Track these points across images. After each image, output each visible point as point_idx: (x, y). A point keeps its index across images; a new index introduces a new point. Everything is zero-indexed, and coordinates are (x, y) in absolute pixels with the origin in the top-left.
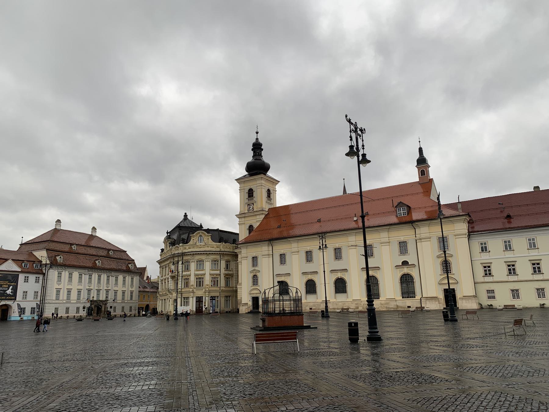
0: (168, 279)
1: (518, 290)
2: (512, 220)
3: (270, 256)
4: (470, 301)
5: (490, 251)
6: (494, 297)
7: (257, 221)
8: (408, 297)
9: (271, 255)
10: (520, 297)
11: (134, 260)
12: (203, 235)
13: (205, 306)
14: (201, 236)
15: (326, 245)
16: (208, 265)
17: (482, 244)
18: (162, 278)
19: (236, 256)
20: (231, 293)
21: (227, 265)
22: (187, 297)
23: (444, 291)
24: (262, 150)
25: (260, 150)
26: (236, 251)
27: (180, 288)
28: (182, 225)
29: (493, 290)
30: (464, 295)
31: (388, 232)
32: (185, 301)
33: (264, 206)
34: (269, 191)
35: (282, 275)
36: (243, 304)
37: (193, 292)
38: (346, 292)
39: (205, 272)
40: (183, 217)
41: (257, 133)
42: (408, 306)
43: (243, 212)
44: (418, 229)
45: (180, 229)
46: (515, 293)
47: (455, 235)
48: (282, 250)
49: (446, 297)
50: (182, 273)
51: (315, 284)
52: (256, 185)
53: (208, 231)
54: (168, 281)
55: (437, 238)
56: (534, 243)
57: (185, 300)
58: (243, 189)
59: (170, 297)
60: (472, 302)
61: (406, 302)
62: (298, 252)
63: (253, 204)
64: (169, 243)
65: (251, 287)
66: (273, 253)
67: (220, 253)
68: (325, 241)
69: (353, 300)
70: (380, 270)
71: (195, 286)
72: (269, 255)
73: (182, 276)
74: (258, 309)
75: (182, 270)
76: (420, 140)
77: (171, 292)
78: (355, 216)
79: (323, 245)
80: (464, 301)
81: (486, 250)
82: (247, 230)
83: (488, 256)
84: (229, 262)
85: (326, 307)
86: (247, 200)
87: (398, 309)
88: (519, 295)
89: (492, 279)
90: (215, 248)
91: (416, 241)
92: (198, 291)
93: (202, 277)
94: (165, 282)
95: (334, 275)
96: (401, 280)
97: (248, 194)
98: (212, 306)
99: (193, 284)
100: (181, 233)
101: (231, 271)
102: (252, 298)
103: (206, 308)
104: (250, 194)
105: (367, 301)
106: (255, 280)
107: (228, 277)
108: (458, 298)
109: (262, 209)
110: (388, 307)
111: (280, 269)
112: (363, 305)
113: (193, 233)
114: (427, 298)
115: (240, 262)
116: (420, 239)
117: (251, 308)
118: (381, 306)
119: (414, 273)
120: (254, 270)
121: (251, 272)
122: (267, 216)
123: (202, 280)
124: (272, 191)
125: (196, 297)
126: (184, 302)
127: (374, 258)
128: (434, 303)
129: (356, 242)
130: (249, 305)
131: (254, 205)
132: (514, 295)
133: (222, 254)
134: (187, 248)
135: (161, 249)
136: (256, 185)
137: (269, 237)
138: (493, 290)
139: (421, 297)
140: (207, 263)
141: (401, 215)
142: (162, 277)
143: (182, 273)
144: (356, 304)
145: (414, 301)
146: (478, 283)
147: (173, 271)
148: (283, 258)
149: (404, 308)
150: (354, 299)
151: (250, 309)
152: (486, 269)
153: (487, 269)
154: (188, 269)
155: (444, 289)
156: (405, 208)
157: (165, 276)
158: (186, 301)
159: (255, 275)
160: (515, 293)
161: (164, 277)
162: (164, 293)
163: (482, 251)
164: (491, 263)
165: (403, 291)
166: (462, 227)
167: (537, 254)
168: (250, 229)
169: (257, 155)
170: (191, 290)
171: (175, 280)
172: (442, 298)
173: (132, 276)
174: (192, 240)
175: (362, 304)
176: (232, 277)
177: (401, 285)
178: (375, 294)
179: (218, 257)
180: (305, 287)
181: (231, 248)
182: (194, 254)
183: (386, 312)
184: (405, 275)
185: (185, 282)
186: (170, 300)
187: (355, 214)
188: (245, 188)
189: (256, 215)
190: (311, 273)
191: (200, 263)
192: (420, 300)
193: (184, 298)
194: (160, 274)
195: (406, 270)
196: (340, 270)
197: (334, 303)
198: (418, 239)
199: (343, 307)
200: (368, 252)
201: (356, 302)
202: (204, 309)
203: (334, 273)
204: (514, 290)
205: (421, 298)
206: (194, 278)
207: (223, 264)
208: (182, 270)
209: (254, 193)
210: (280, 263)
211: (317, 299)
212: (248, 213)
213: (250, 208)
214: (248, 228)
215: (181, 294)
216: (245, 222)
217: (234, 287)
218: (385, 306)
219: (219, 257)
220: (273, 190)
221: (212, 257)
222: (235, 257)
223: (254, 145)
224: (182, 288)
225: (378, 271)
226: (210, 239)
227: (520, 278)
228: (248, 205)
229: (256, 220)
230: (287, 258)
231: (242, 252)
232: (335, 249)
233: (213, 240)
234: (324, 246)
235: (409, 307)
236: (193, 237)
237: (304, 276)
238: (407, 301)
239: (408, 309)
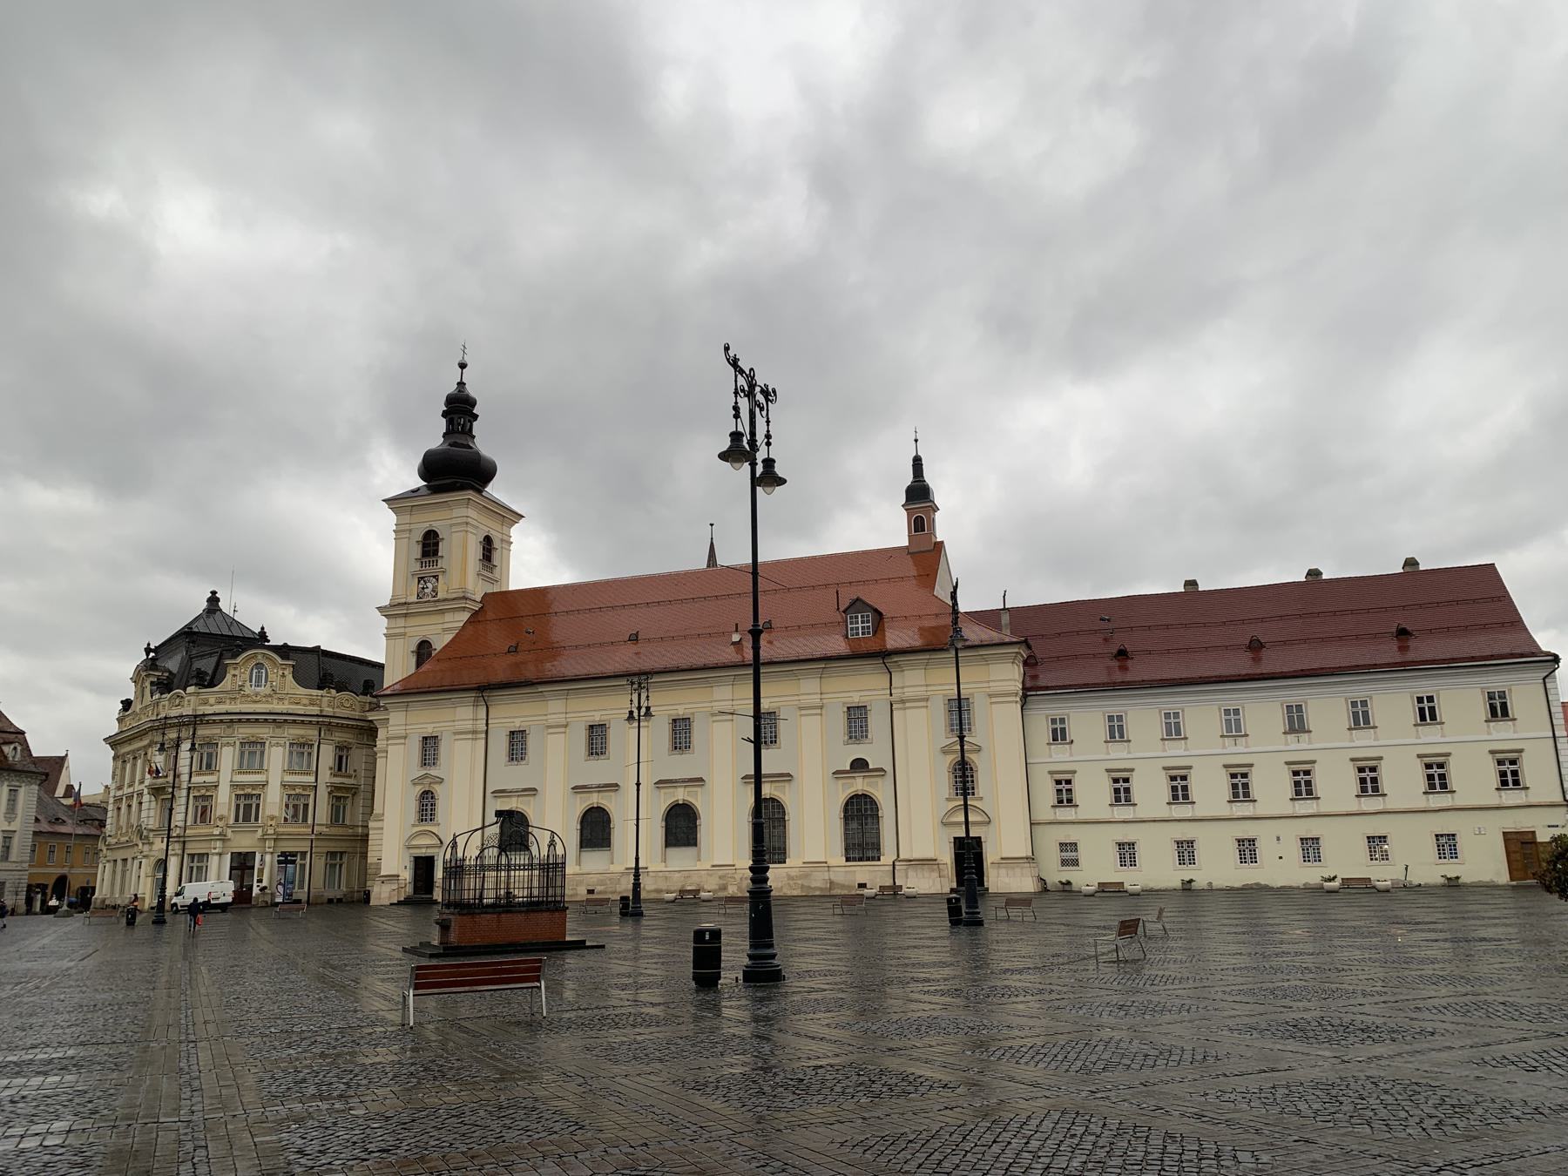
0: (140, 794)
1: (1253, 841)
2: (1129, 663)
3: (479, 736)
4: (1018, 870)
5: (1072, 741)
6: (1075, 862)
7: (444, 630)
8: (861, 859)
9: (481, 732)
10: (1137, 863)
11: (23, 733)
12: (267, 664)
13: (260, 881)
14: (259, 666)
15: (648, 708)
16: (276, 758)
17: (1054, 721)
18: (120, 793)
19: (369, 732)
20: (344, 844)
21: (341, 758)
22: (203, 854)
23: (955, 843)
24: (475, 417)
25: (468, 418)
26: (371, 716)
27: (181, 824)
28: (200, 628)
29: (1076, 844)
30: (1004, 856)
31: (820, 678)
32: (195, 864)
33: (470, 587)
34: (488, 540)
35: (511, 792)
36: (383, 876)
37: (223, 838)
38: (695, 845)
39: (267, 777)
40: (204, 605)
41: (463, 366)
42: (859, 884)
43: (403, 601)
44: (897, 673)
45: (193, 642)
46: (1127, 853)
47: (990, 696)
48: (515, 720)
49: (959, 859)
50: (191, 777)
51: (609, 821)
52: (450, 522)
53: (285, 651)
54: (141, 803)
55: (944, 700)
56: (1177, 724)
57: (193, 862)
58: (407, 530)
59: (145, 854)
60: (1022, 874)
61: (855, 871)
62: (566, 726)
63: (434, 577)
64: (152, 683)
65: (413, 825)
66: (490, 726)
67: (318, 722)
68: (648, 697)
69: (713, 866)
70: (793, 783)
71: (232, 821)
72: (474, 732)
73: (189, 788)
74: (431, 893)
76: (918, 438)
77: (147, 837)
78: (737, 631)
79: (639, 708)
80: (1003, 871)
81: (1064, 738)
83: (1068, 754)
84: (348, 749)
85: (637, 885)
86: (419, 564)
87: (834, 892)
88: (1257, 852)
89: (1073, 813)
90: (305, 705)
91: (892, 705)
92: (238, 836)
93: (254, 792)
94: (129, 806)
95: (665, 793)
96: (846, 810)
97: (420, 546)
98: (282, 881)
99: (225, 813)
100: (194, 652)
101: (350, 777)
102: (412, 859)
103: (263, 889)
104: (429, 545)
105: (751, 869)
106: (427, 805)
107: (341, 796)
108: (989, 862)
109: (462, 595)
110: (806, 884)
111: (507, 776)
112: (741, 879)
113: (235, 656)
114: (910, 861)
115: (382, 752)
116: (903, 702)
117: (409, 890)
118: (789, 884)
119: (881, 792)
120: (426, 776)
121: (415, 783)
122: (476, 617)
123: (254, 802)
124: (496, 544)
125: (232, 853)
126: (192, 868)
127: (872, 743)
128: (926, 874)
129: (734, 703)
130: (400, 881)
131: (437, 580)
132: (1183, 856)
133: (325, 724)
134: (212, 701)
135: (122, 702)
136: (450, 522)
137: (481, 678)
138: (1076, 844)
139: (896, 858)
141: (857, 634)
142: (120, 788)
143: (191, 777)
144: (720, 878)
145: (876, 868)
146: (1039, 824)
147: (158, 771)
148: (517, 743)
149: (849, 887)
150: (715, 863)
151: (405, 891)
152: (1060, 787)
153: (1064, 786)
154: (210, 766)
155: (955, 838)
156: (868, 616)
157: (130, 786)
158: (197, 867)
159: (426, 792)
160: (1127, 853)
161: (127, 790)
162: (124, 839)
163: (1055, 739)
164: (1075, 772)
165: (850, 841)
166: (1008, 674)
167: (1182, 752)
168: (422, 651)
169: (458, 432)
170: (217, 831)
171: (163, 799)
172: (949, 862)
173: (13, 783)
174: (229, 677)
175: (738, 877)
176: (353, 795)
177: (846, 824)
178: (774, 849)
179: (312, 733)
180: (579, 827)
181: (358, 707)
182: (234, 720)
183: (802, 899)
184: (856, 796)
185: (197, 807)
186: (143, 861)
187: (737, 625)
188: (412, 526)
189: (442, 612)
190: (599, 787)
191: (252, 751)
192: (891, 868)
193: (192, 856)
194: (113, 778)
195: (859, 784)
196: (684, 781)
197: (661, 874)
198: (897, 702)
199: (683, 886)
200: (763, 732)
201: (720, 873)
202: (256, 891)
203: (666, 790)
204: (1243, 841)
205: (894, 862)
206: (230, 797)
207: (327, 755)
208: (191, 768)
209: (440, 544)
210: (507, 758)
211: (612, 863)
212: (417, 603)
213: (426, 590)
215: (182, 845)
216: (407, 630)
217: (358, 826)
218: (799, 882)
219: (316, 733)
220: (502, 540)
221: (291, 731)
222: (368, 736)
223: (450, 400)
224: (188, 824)
225: (787, 784)
226: (290, 677)
227: (1391, 803)
228: (420, 579)
229: (440, 626)
230: (532, 743)
231: (391, 722)
232: (674, 721)
233: (300, 679)
234: (643, 711)
235: (863, 886)
236: (235, 669)
237: (579, 796)
238: (859, 868)
239: (858, 892)
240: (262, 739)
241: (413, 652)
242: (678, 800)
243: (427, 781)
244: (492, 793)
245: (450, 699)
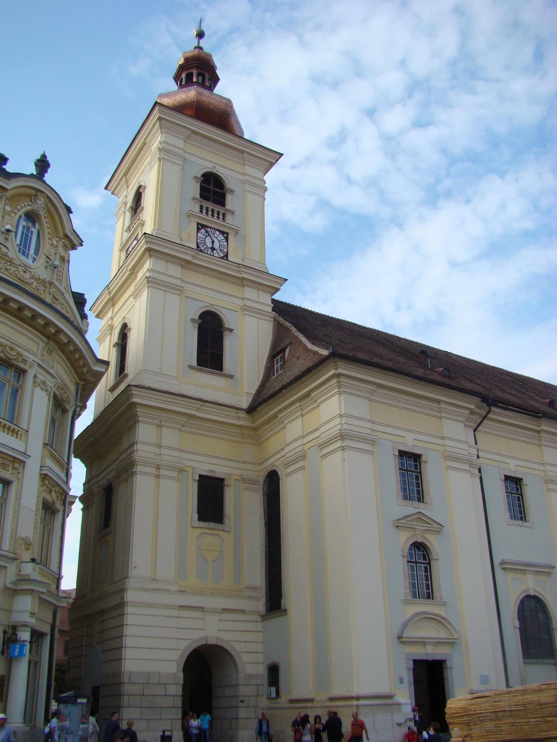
52: (242, 178)
63: (222, 233)
72: (471, 464)
82: (190, 324)
102: (411, 665)
131: (227, 239)
136: (242, 178)
140: (38, 390)
189: (242, 282)
214: (197, 318)
228: (200, 227)
229: (240, 303)
240: (25, 361)
241: (193, 320)
243: (420, 526)
245: (438, 402)
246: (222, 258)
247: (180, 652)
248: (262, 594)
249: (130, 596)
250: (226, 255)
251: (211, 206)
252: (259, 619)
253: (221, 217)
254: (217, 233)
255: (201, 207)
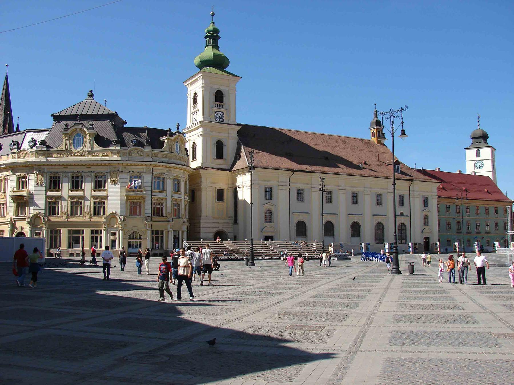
40: (87, 97)
63: (222, 112)
73: (152, 198)
75: (152, 188)
131: (224, 114)
148: (301, 195)
209: (224, 97)
228: (216, 112)
242: (354, 221)
244: (293, 213)
246: (222, 121)
247: (213, 233)
248: (233, 219)
249: (202, 221)
250: (224, 120)
251: (218, 103)
252: (232, 225)
253: (222, 106)
254: (221, 112)
255: (216, 104)
